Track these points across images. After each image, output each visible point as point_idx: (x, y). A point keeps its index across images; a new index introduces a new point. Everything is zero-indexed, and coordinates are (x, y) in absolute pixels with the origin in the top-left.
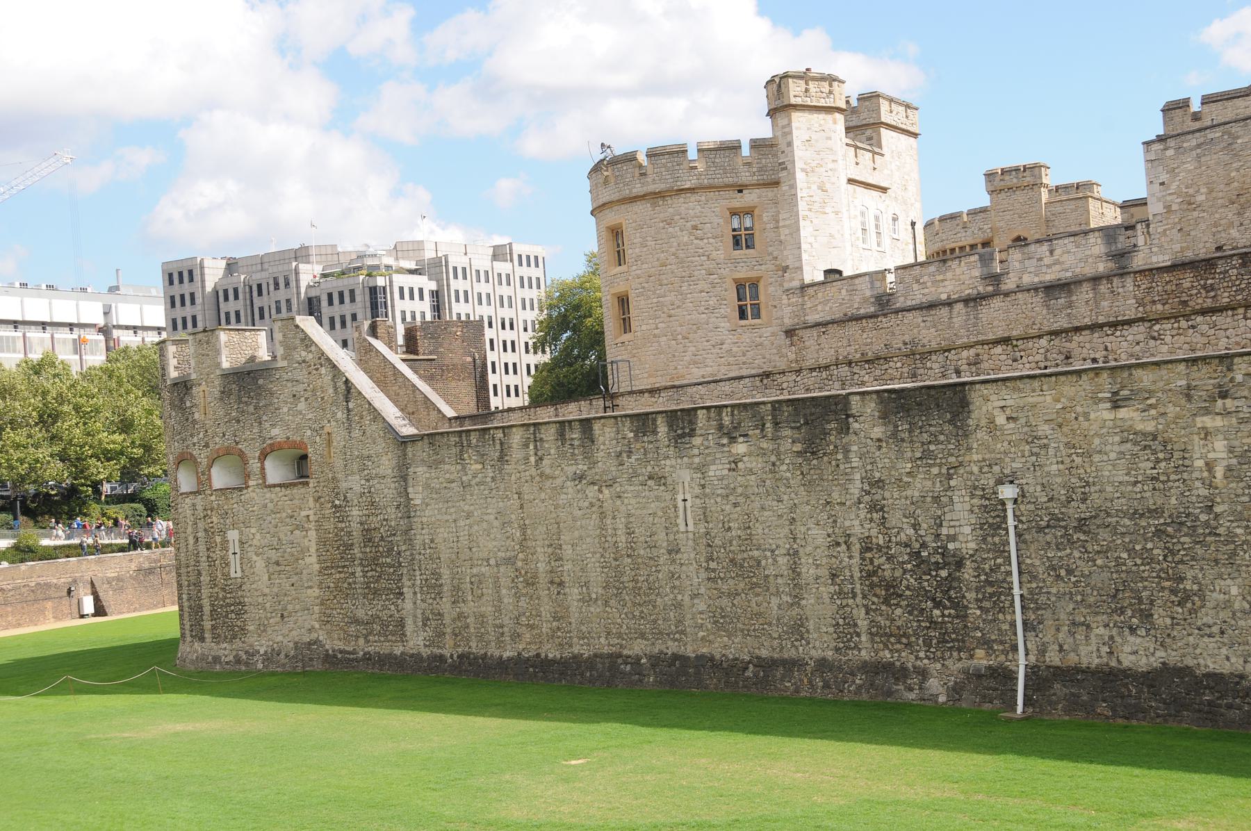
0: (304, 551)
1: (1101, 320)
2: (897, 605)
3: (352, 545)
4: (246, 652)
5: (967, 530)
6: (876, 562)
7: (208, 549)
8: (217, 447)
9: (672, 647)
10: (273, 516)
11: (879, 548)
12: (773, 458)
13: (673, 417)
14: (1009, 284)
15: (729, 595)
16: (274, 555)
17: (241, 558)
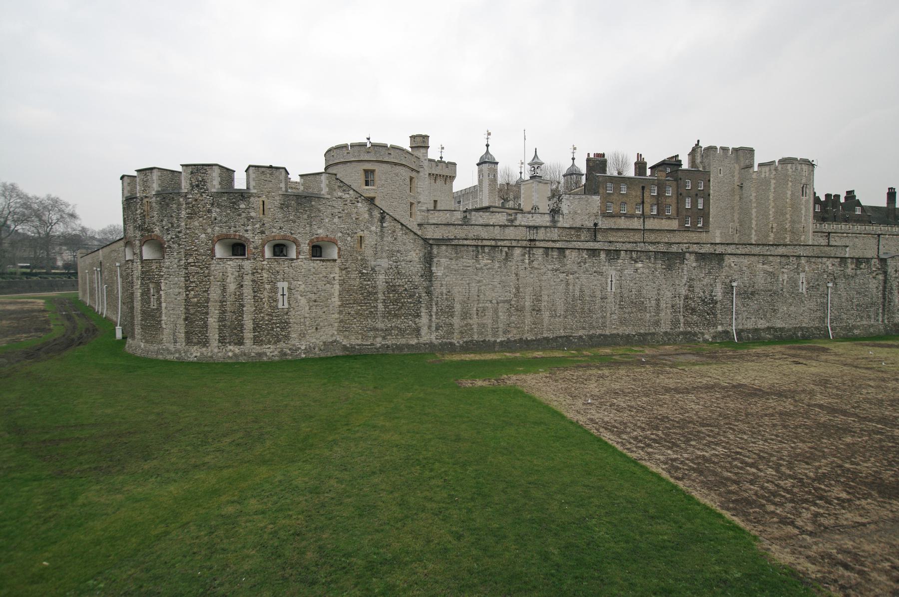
0: (332, 295)
1: (547, 239)
2: (695, 315)
3: (376, 293)
4: (290, 349)
5: (720, 294)
6: (689, 303)
7: (254, 292)
8: (273, 234)
9: (599, 332)
10: (315, 276)
11: (691, 298)
12: (653, 269)
13: (608, 252)
14: (517, 223)
15: (628, 313)
16: (313, 297)
17: (289, 298)
